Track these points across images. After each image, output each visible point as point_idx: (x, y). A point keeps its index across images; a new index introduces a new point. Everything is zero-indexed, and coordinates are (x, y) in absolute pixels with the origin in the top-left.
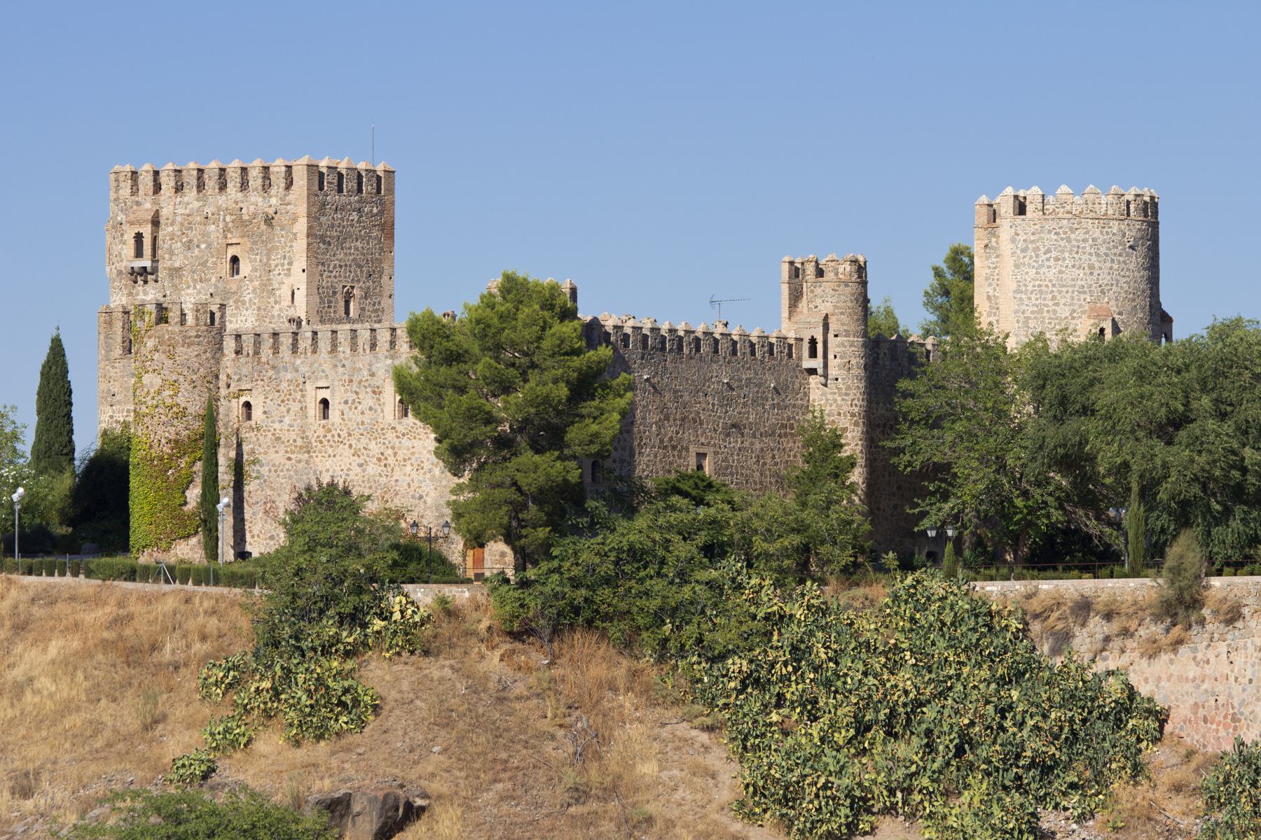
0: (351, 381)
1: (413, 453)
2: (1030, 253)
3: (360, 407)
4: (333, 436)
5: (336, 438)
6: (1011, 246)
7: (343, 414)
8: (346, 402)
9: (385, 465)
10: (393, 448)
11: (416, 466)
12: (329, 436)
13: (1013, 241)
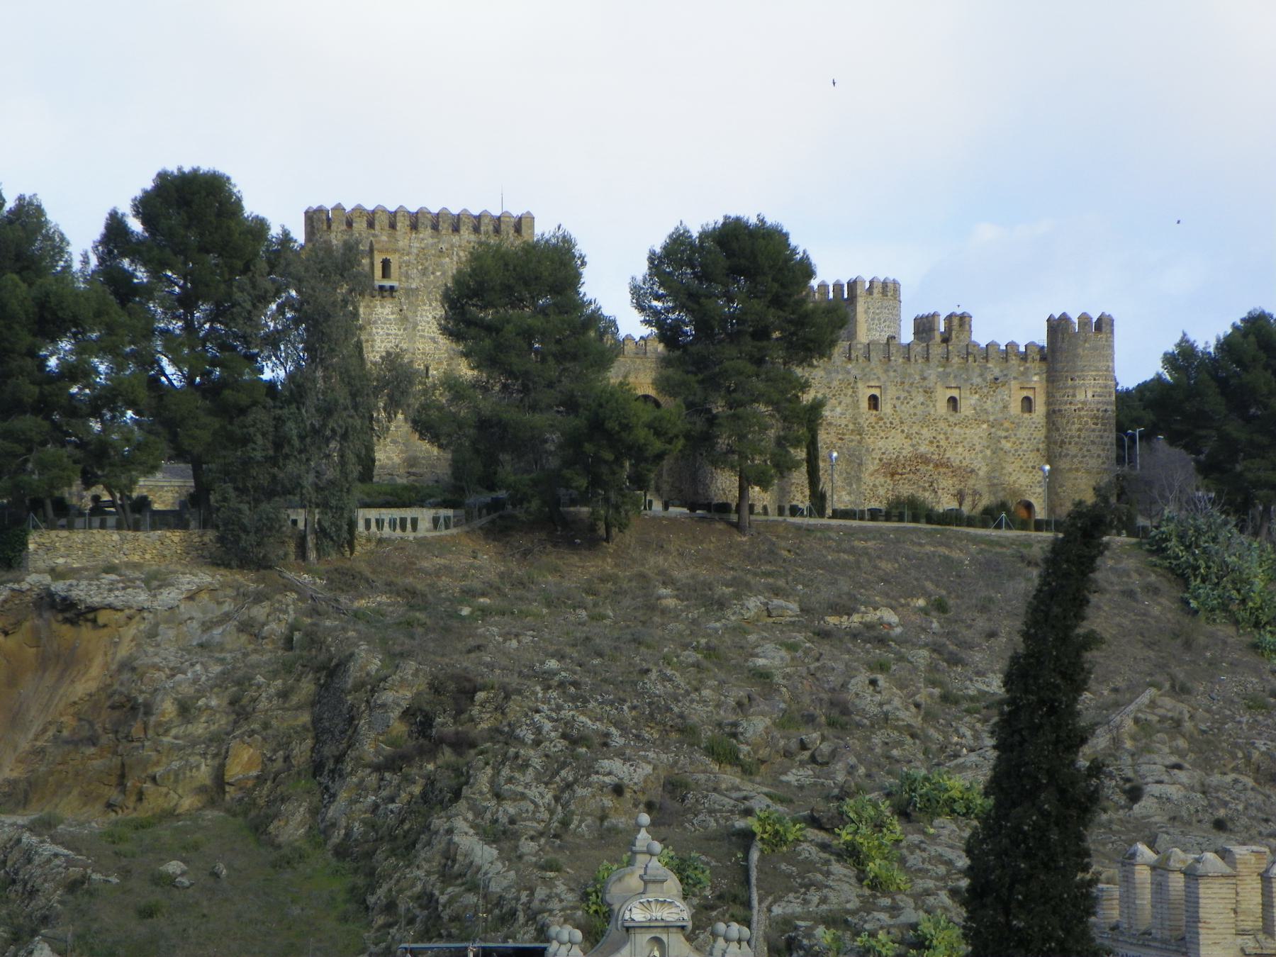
0: (903, 383)
1: (965, 438)
2: (876, 322)
3: (912, 403)
4: (885, 423)
5: (889, 425)
6: (864, 316)
7: (895, 407)
8: (898, 398)
9: (937, 446)
10: (945, 434)
11: (967, 449)
12: (881, 423)
13: (866, 312)
